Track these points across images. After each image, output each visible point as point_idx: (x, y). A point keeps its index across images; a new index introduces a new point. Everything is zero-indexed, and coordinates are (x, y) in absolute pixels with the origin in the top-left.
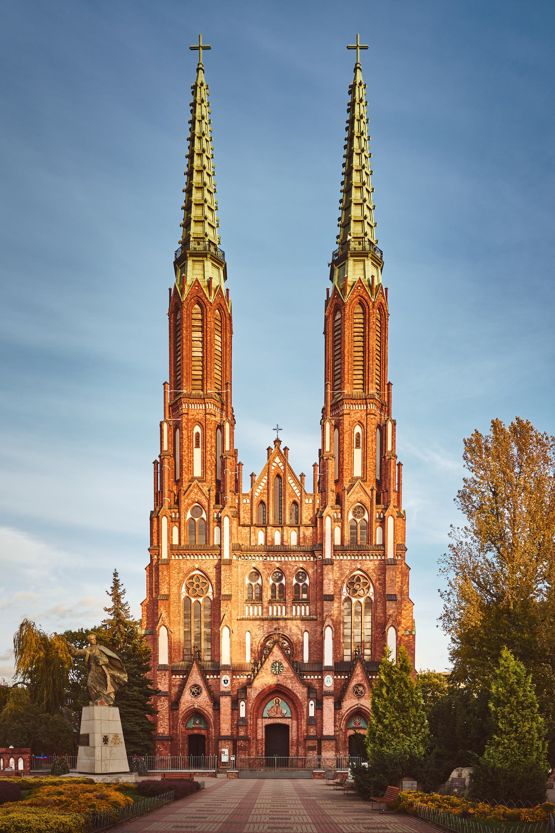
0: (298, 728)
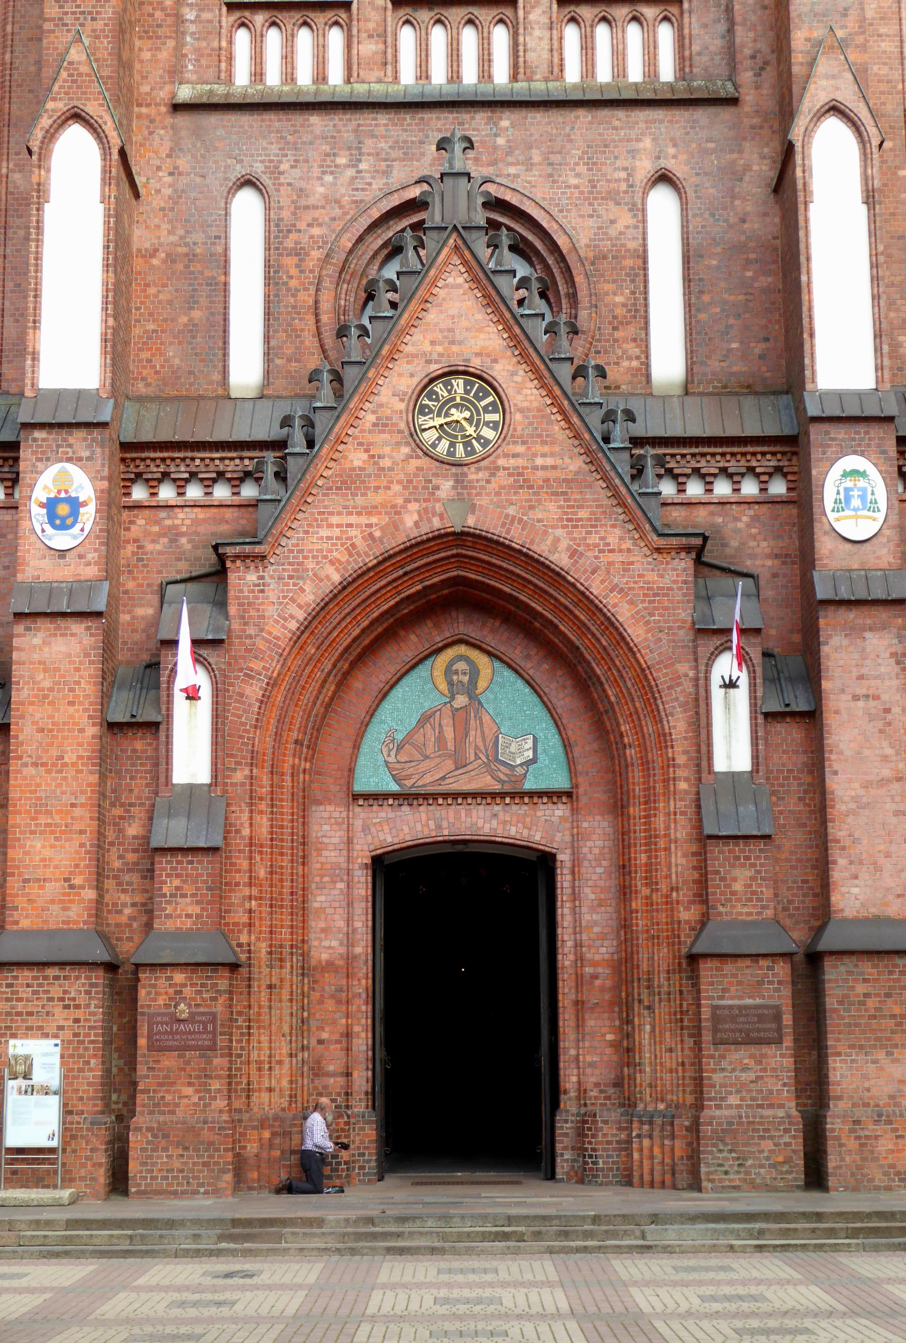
0: (624, 868)
